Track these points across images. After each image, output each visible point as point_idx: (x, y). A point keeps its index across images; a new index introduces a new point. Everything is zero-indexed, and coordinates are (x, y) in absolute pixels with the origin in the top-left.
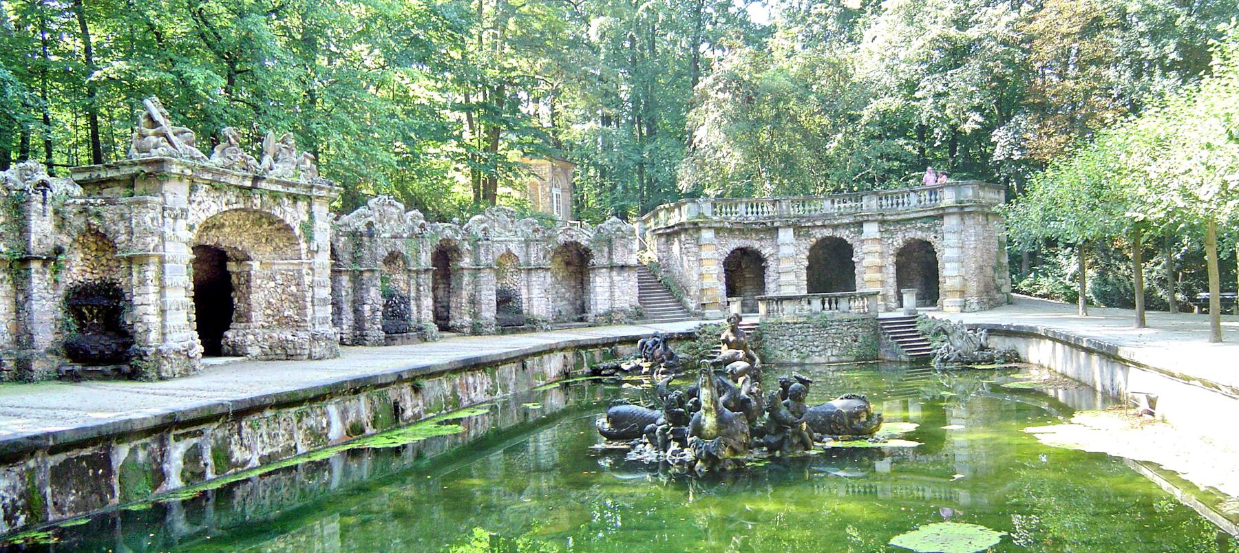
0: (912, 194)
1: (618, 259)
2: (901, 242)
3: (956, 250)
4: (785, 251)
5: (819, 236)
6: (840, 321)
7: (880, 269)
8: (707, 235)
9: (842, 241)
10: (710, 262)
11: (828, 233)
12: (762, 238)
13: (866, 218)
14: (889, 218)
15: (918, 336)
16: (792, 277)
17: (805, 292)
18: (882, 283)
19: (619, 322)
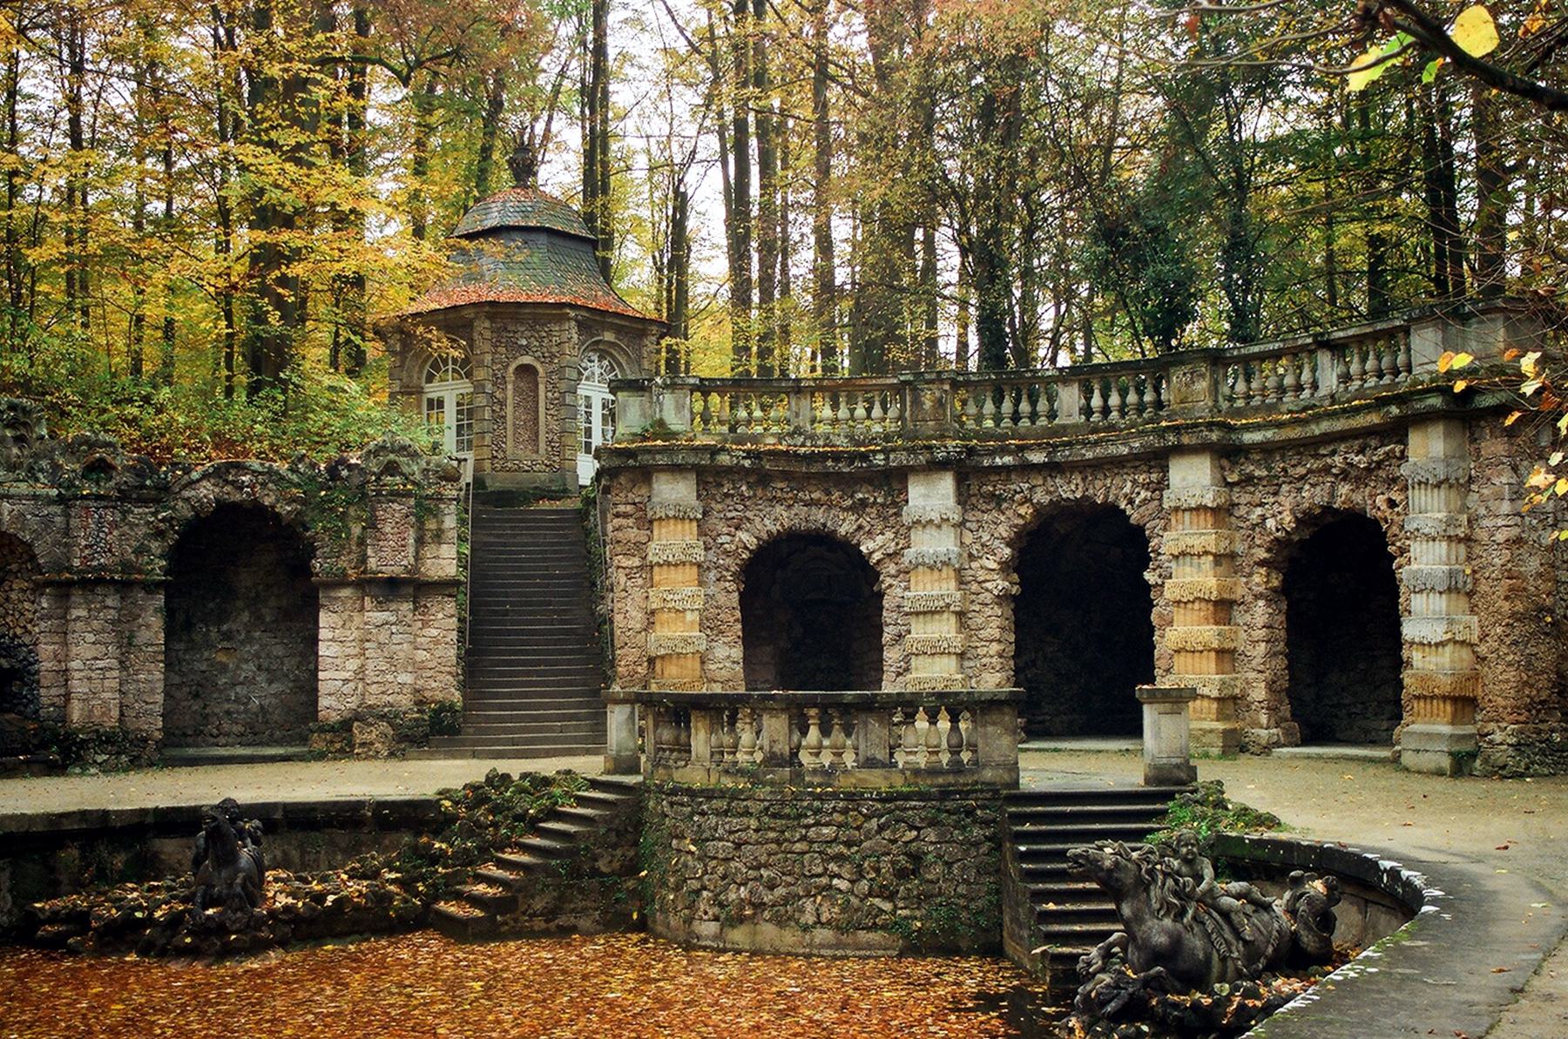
0: (1324, 358)
1: (387, 559)
2: (1287, 518)
3: (1442, 548)
4: (935, 544)
5: (1040, 497)
6: (850, 797)
7: (1223, 608)
8: (675, 491)
9: (1112, 513)
10: (676, 575)
11: (1070, 489)
12: (863, 504)
13: (1172, 439)
14: (1249, 437)
15: (1061, 876)
16: (944, 629)
17: (993, 680)
18: (1226, 656)
19: (368, 753)
